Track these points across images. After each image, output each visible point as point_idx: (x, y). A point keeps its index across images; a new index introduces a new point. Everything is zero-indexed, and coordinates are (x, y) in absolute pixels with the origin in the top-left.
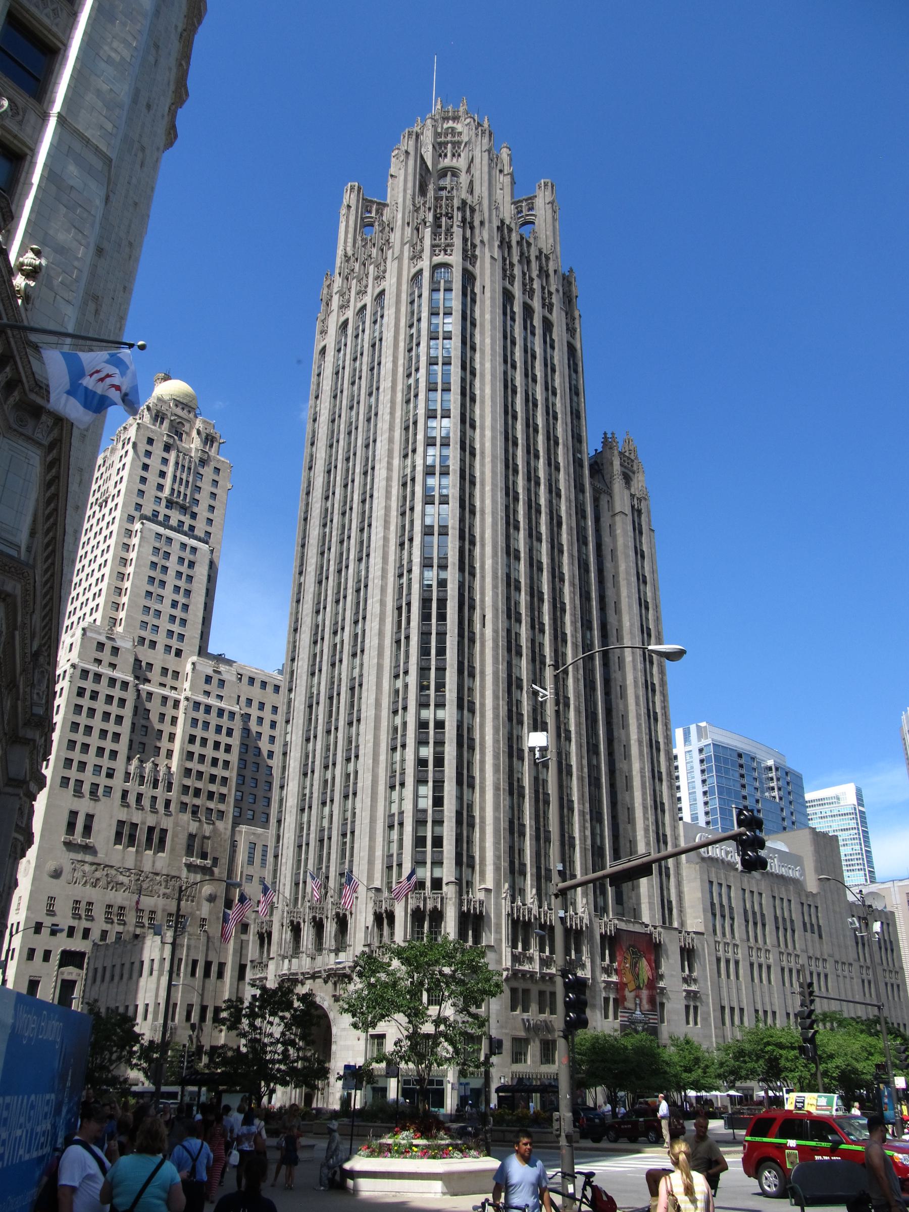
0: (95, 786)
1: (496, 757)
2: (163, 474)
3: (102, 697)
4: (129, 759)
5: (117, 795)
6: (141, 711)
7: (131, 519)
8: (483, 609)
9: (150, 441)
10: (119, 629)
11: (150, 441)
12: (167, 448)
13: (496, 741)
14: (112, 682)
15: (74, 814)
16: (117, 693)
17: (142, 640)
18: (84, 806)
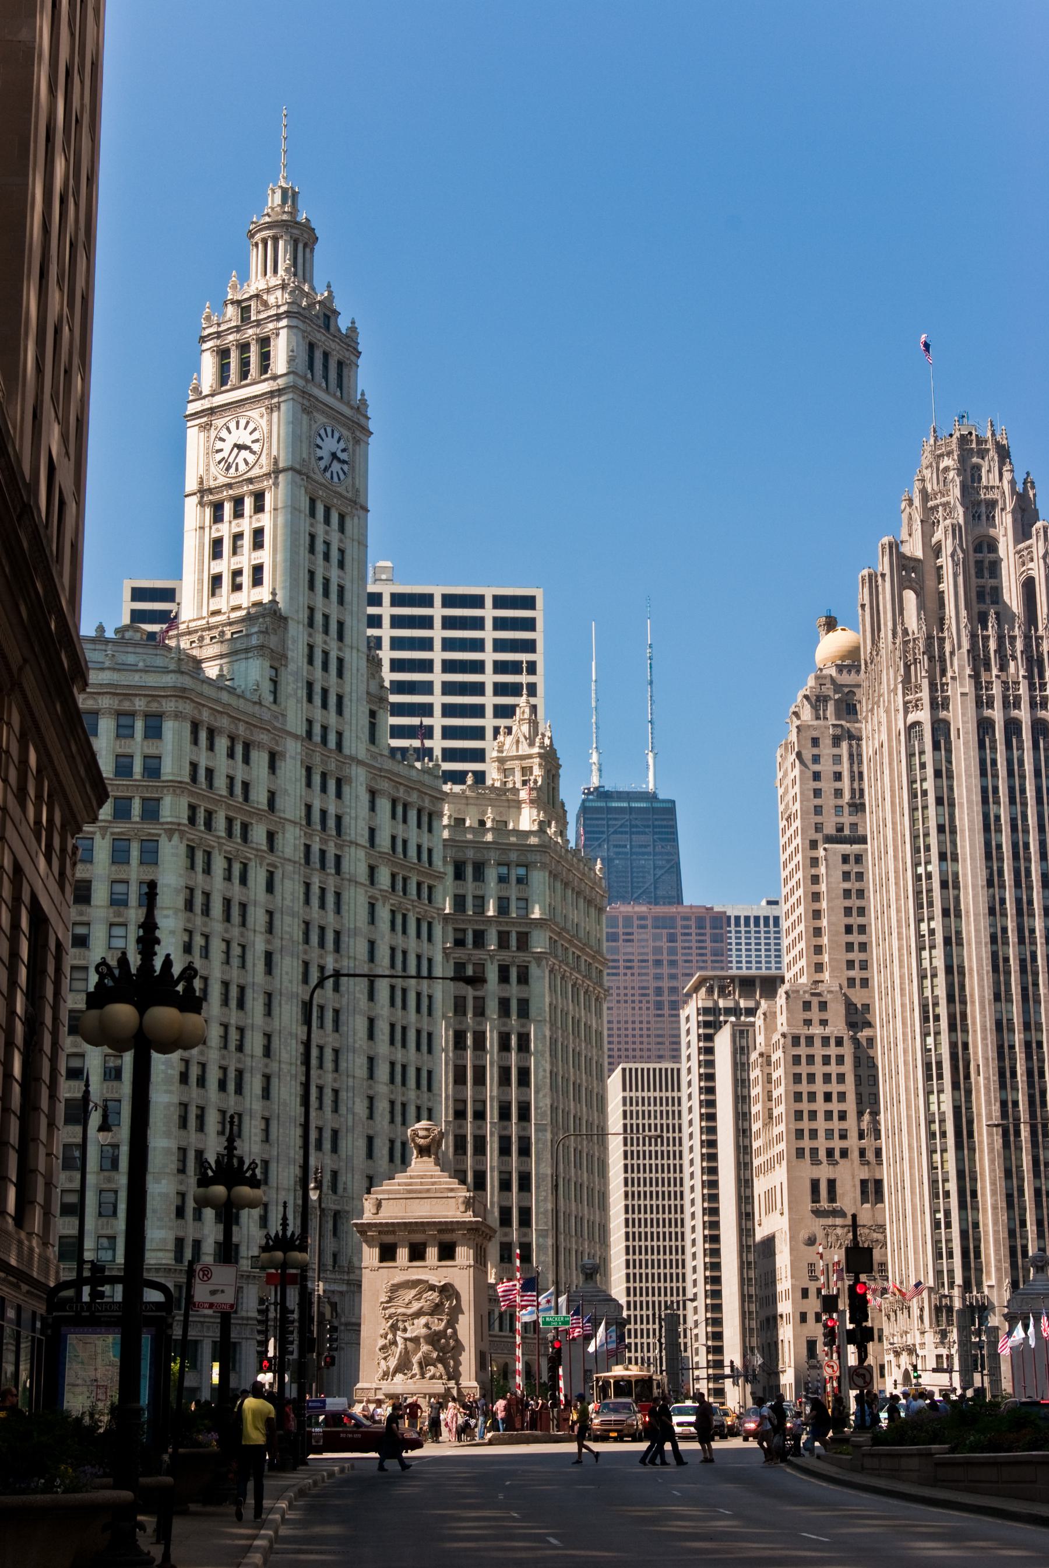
0: (830, 1153)
1: (993, 1183)
2: (838, 776)
3: (818, 1060)
4: (860, 1114)
5: (855, 1155)
6: (864, 1061)
7: (814, 845)
8: (976, 1060)
9: (815, 742)
10: (826, 975)
11: (815, 742)
12: (836, 741)
13: (992, 1171)
14: (826, 1041)
15: (815, 1184)
16: (833, 1051)
17: (851, 982)
18: (824, 1172)
